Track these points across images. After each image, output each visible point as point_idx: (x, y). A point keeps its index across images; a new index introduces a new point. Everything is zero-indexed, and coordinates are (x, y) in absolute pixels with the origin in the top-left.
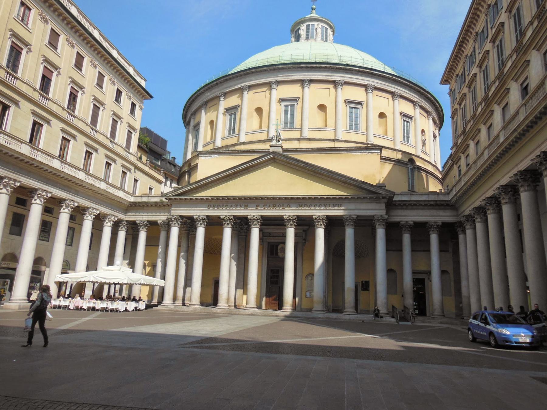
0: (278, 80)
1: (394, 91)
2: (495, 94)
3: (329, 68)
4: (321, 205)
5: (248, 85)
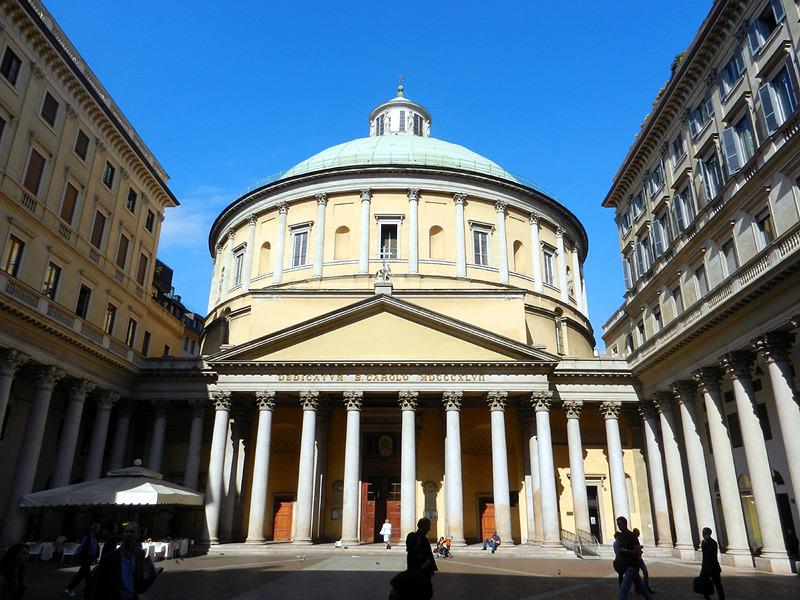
2: (710, 225)
3: (446, 175)
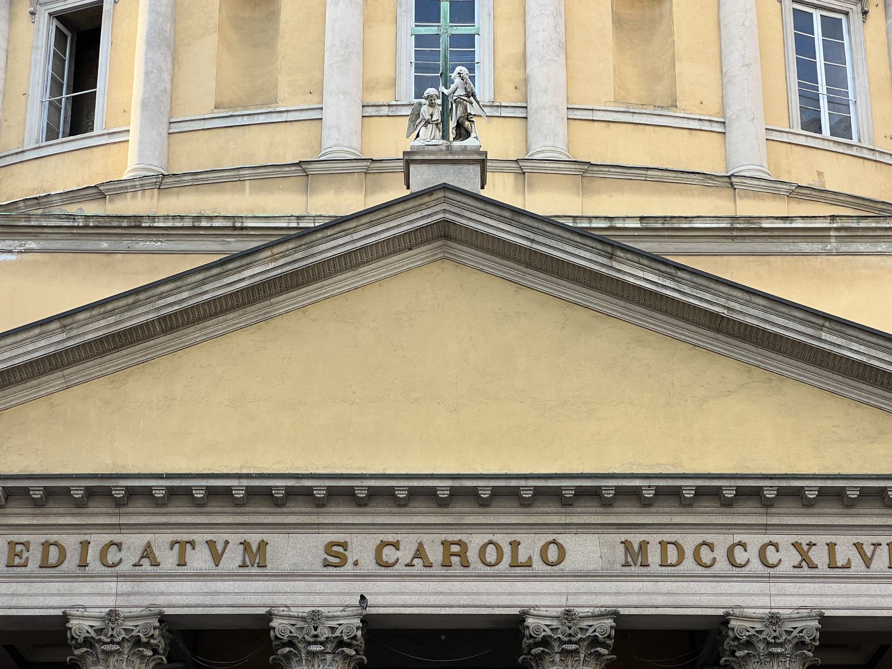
4: (776, 546)
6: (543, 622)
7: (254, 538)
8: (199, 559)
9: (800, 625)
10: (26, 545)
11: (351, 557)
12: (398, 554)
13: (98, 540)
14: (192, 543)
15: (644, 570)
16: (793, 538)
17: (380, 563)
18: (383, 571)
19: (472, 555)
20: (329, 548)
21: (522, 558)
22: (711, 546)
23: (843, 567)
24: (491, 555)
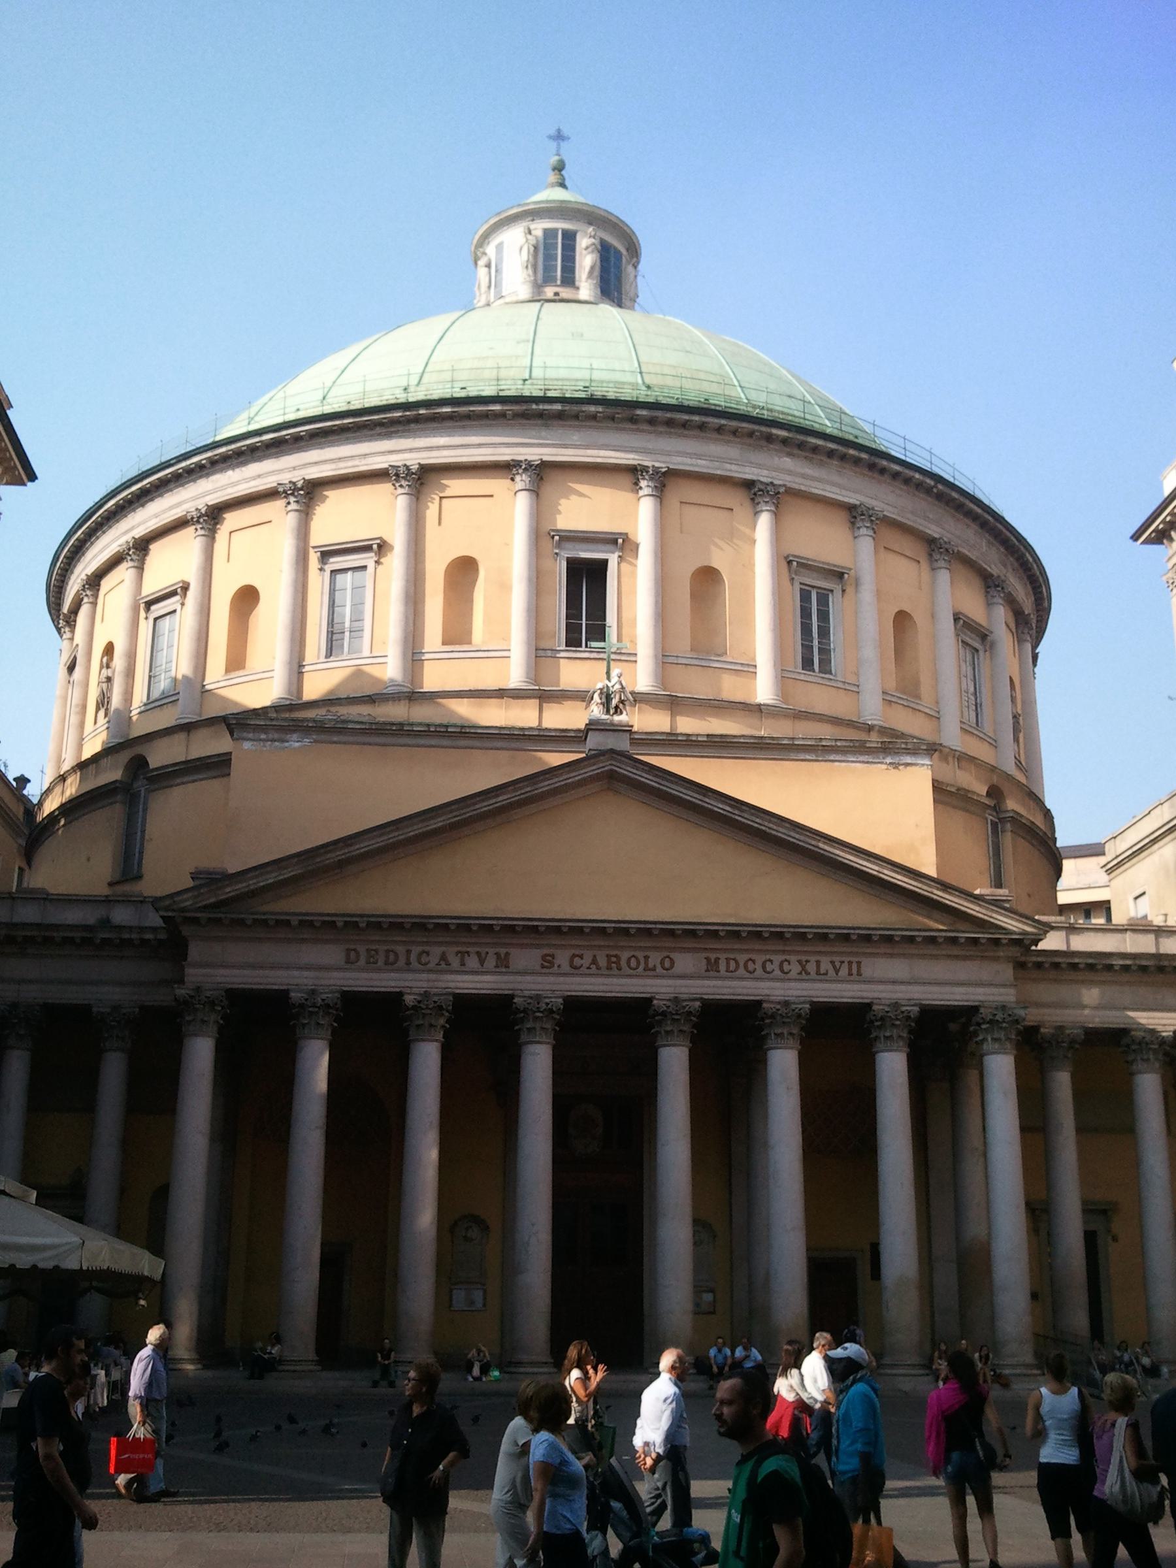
0: (545, 458)
1: (936, 536)
5: (423, 462)
6: (662, 1003)
7: (503, 951)
8: (472, 962)
9: (800, 1006)
10: (376, 951)
11: (557, 962)
12: (582, 962)
13: (416, 950)
14: (468, 953)
15: (716, 974)
16: (799, 958)
17: (572, 966)
18: (576, 972)
19: (623, 963)
20: (544, 957)
21: (651, 965)
22: (754, 962)
23: (824, 974)
24: (633, 963)
